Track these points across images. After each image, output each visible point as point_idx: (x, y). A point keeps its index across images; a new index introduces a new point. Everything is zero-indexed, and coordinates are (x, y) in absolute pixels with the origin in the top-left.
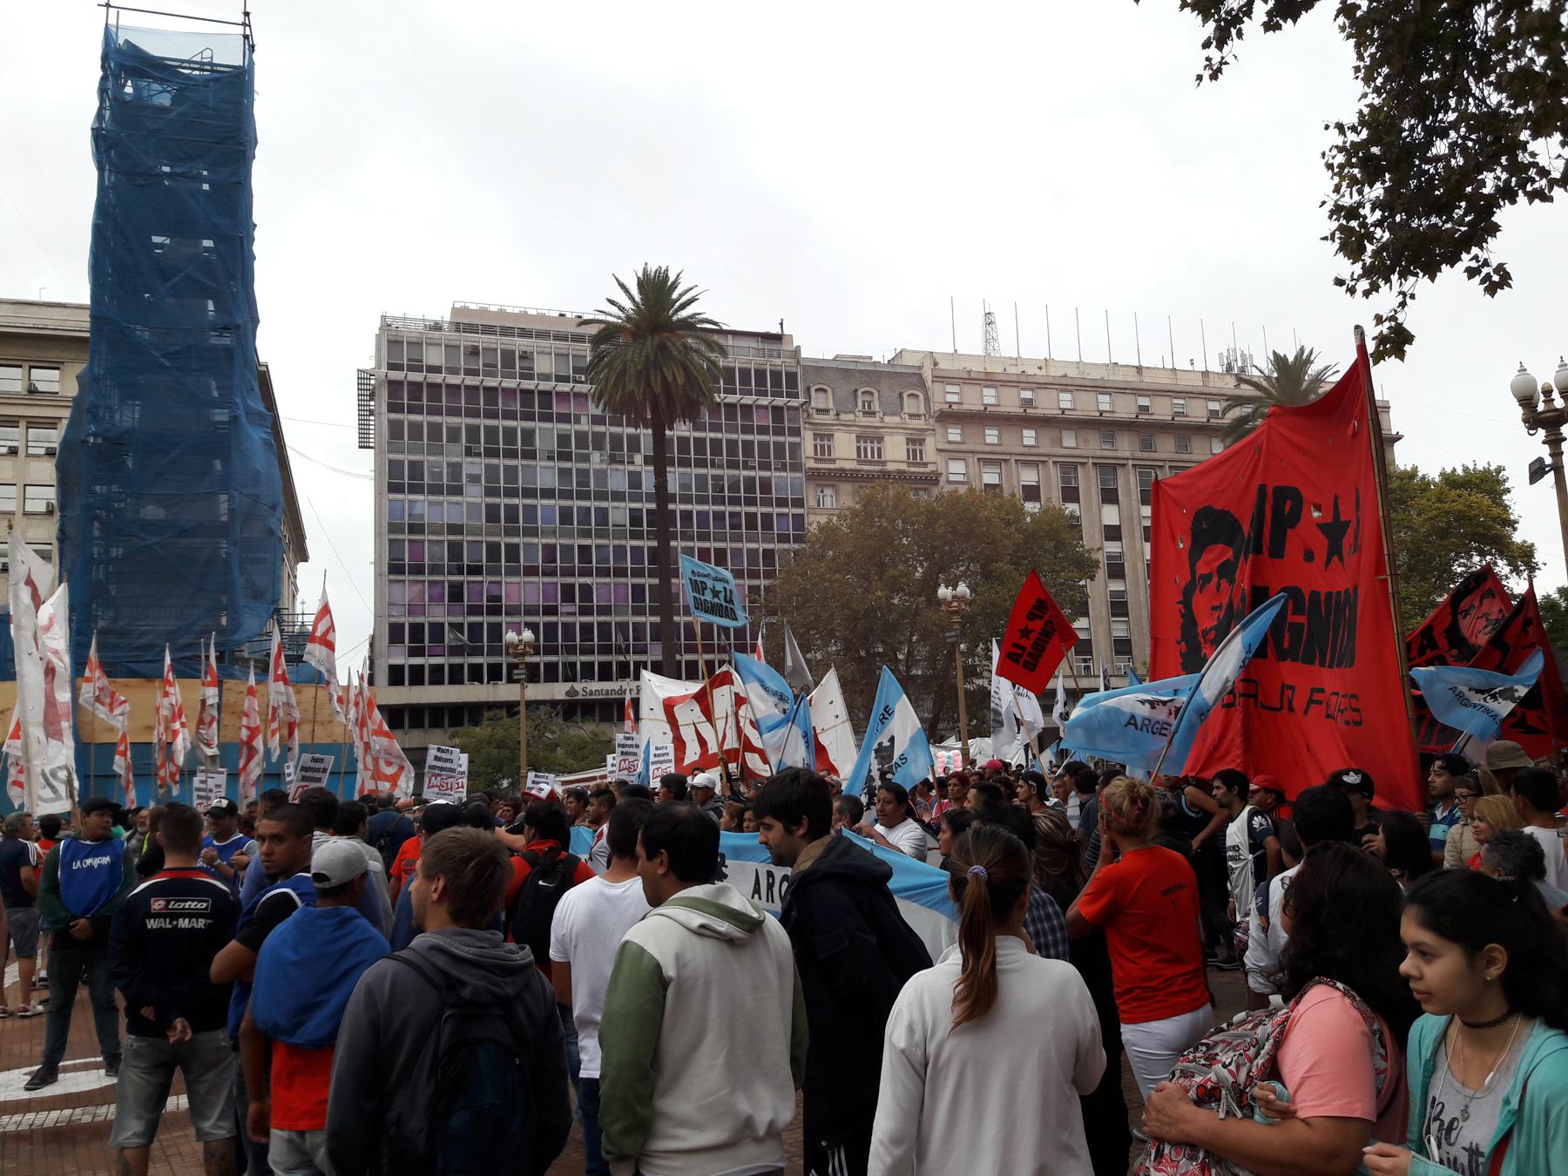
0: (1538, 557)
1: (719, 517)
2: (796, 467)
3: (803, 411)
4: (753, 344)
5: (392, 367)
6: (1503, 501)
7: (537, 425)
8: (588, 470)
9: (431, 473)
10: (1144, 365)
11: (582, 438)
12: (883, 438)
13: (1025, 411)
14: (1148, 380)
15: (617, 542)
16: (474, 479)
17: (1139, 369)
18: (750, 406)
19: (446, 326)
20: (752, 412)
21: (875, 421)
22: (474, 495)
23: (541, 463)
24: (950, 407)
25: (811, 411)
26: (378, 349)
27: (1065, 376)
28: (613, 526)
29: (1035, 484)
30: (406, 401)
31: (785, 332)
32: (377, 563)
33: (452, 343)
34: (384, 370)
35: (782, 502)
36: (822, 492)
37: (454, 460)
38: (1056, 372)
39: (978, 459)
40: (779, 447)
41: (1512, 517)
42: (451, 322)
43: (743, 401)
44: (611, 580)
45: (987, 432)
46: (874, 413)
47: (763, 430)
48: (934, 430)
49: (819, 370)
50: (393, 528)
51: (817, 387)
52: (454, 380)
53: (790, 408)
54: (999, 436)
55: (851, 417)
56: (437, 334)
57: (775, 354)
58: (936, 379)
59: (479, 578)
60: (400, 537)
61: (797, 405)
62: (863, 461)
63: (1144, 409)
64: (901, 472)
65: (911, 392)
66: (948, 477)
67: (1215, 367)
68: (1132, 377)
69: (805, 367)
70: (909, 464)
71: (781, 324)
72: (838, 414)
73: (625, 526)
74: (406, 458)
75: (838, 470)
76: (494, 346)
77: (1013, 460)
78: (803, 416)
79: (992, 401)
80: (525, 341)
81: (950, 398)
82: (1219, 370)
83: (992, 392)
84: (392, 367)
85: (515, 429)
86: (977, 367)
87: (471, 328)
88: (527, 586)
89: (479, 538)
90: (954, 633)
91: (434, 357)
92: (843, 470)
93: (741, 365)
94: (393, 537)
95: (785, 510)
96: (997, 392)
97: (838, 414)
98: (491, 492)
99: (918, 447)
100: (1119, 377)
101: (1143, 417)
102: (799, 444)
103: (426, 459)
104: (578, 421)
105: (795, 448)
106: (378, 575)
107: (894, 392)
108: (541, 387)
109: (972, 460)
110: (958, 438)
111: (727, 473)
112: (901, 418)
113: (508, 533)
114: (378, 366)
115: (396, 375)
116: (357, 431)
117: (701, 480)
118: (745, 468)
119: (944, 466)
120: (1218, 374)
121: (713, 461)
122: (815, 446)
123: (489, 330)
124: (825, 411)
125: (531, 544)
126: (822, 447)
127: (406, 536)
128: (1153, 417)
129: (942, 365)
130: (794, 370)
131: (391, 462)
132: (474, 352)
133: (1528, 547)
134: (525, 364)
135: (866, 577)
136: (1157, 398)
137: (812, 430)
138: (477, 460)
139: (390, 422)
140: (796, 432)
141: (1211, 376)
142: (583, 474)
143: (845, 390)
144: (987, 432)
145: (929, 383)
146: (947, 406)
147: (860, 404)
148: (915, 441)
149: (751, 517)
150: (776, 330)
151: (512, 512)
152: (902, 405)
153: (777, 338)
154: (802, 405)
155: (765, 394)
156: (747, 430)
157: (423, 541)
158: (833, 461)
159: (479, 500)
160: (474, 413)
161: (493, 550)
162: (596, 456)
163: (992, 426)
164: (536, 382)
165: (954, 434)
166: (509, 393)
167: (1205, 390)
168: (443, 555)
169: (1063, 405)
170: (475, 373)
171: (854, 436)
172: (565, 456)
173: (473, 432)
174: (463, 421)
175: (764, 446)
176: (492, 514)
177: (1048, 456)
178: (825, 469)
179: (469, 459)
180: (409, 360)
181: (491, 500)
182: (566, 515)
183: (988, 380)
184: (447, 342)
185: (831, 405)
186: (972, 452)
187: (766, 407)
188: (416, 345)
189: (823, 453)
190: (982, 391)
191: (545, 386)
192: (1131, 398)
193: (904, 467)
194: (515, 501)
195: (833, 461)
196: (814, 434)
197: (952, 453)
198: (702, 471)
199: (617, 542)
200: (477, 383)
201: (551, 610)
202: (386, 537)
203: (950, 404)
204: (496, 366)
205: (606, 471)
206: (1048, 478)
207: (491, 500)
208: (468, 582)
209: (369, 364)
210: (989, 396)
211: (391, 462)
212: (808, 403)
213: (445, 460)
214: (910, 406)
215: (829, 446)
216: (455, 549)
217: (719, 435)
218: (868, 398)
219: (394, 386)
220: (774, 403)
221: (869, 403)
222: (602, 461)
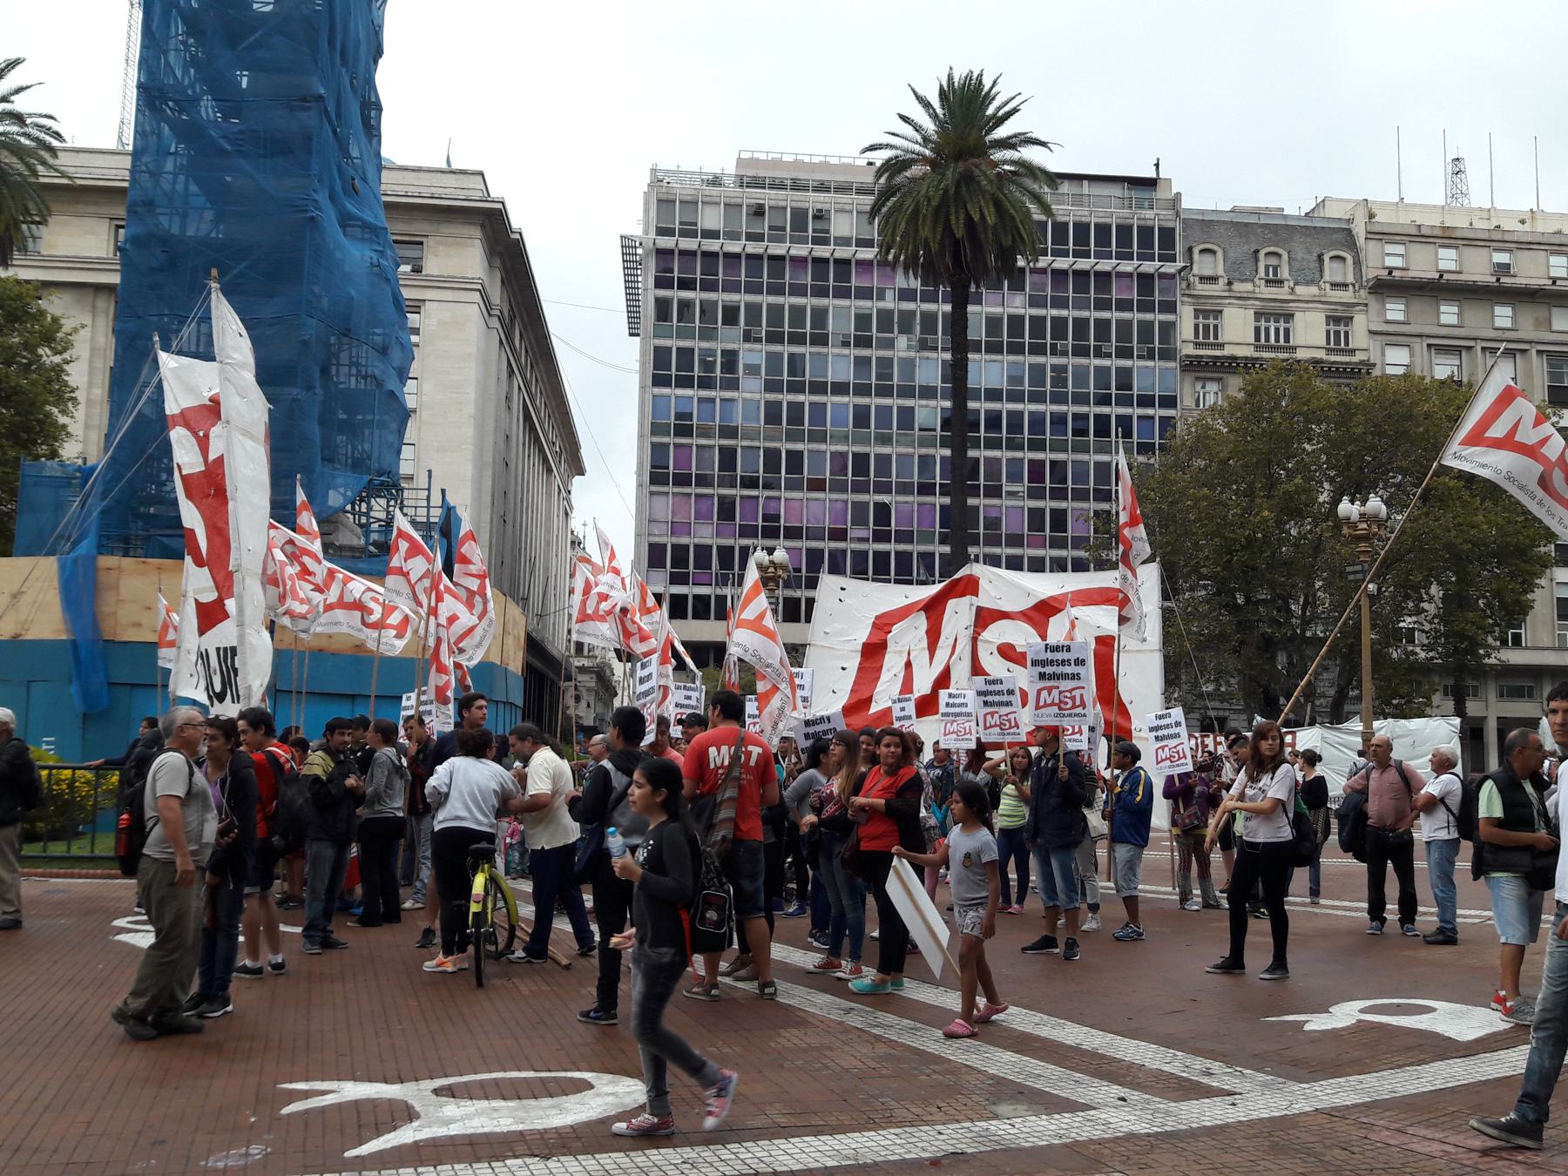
1: (1058, 420)
2: (1168, 354)
4: (1115, 191)
5: (661, 232)
7: (830, 302)
8: (891, 360)
9: (703, 362)
11: (885, 318)
12: (1293, 315)
13: (1498, 280)
15: (924, 451)
16: (752, 370)
18: (1107, 275)
19: (729, 181)
20: (1110, 282)
21: (1282, 293)
22: (751, 391)
23: (832, 350)
24: (1390, 273)
25: (1192, 279)
26: (646, 211)
27: (1559, 233)
28: (921, 430)
30: (698, 276)
32: (639, 473)
33: (733, 201)
34: (652, 235)
35: (1146, 401)
36: (1203, 387)
37: (730, 346)
38: (1544, 227)
39: (1429, 346)
40: (1146, 327)
42: (736, 176)
43: (1099, 268)
44: (914, 499)
45: (1443, 308)
46: (1281, 282)
47: (1124, 305)
48: (1366, 305)
49: (1208, 226)
50: (656, 429)
52: (734, 247)
53: (1163, 276)
54: (1460, 315)
55: (1248, 286)
56: (714, 191)
57: (1146, 204)
59: (754, 493)
60: (665, 440)
61: (1172, 270)
64: (1316, 362)
66: (1384, 369)
70: (1329, 351)
72: (1230, 283)
73: (934, 430)
74: (674, 343)
75: (1228, 358)
76: (783, 204)
77: (1479, 348)
78: (1180, 286)
79: (1452, 266)
80: (822, 196)
81: (1391, 262)
83: (1452, 253)
84: (661, 232)
85: (803, 308)
86: (1431, 221)
87: (757, 183)
88: (811, 503)
89: (756, 444)
90: (1359, 568)
91: (711, 219)
92: (1234, 358)
94: (657, 439)
95: (1150, 412)
97: (1230, 283)
98: (772, 386)
99: (1342, 328)
102: (1173, 324)
103: (697, 344)
104: (881, 297)
105: (1168, 329)
106: (640, 485)
107: (1311, 253)
108: (838, 255)
109: (1420, 346)
110: (1400, 317)
111: (1071, 361)
112: (1320, 288)
113: (791, 437)
114: (646, 232)
115: (666, 242)
116: (625, 315)
117: (1037, 371)
118: (1098, 354)
119: (1379, 353)
121: (1054, 346)
122: (1196, 326)
123: (778, 185)
124: (1213, 279)
125: (818, 451)
126: (1206, 327)
127: (671, 440)
129: (1376, 219)
130: (1170, 225)
131: (657, 349)
132: (758, 212)
134: (820, 226)
135: (1250, 493)
137: (1191, 304)
138: (757, 346)
139: (658, 300)
140: (1170, 307)
142: (885, 364)
143: (1241, 250)
144: (1443, 308)
145: (1361, 241)
146: (1386, 272)
148: (1339, 319)
149: (1103, 421)
150: (1150, 173)
151: (796, 410)
152: (1322, 271)
153: (1150, 183)
154: (1180, 271)
155: (1129, 257)
156: (1103, 305)
157: (690, 446)
159: (757, 396)
160: (754, 288)
161: (772, 457)
162: (902, 342)
163: (1449, 300)
164: (832, 247)
165: (1395, 310)
166: (799, 262)
168: (714, 463)
169: (1554, 273)
170: (757, 238)
171: (1252, 312)
172: (862, 342)
173: (754, 311)
174: (742, 299)
175: (1124, 326)
176: (773, 413)
177: (1530, 342)
178: (1209, 357)
179: (747, 346)
180: (681, 223)
181: (771, 397)
182: (861, 417)
183: (1447, 237)
184: (728, 201)
185: (1220, 271)
186: (1420, 336)
187: (1130, 275)
188: (691, 204)
189: (1207, 335)
191: (843, 253)
193: (1321, 355)
194: (800, 398)
195: (1221, 346)
196: (1195, 310)
197: (1390, 336)
198: (1040, 359)
199: (924, 451)
200: (761, 251)
201: (838, 535)
202: (649, 439)
203: (1391, 271)
204: (784, 229)
205: (913, 360)
206: (1529, 374)
207: (771, 397)
208: (742, 497)
209: (636, 230)
210: (1447, 259)
211: (657, 349)
212: (1188, 268)
213: (718, 346)
214: (1332, 271)
215: (1216, 327)
216: (728, 456)
217: (1064, 313)
218: (1273, 261)
219: (663, 254)
220: (1141, 269)
221: (1275, 269)
222: (909, 347)
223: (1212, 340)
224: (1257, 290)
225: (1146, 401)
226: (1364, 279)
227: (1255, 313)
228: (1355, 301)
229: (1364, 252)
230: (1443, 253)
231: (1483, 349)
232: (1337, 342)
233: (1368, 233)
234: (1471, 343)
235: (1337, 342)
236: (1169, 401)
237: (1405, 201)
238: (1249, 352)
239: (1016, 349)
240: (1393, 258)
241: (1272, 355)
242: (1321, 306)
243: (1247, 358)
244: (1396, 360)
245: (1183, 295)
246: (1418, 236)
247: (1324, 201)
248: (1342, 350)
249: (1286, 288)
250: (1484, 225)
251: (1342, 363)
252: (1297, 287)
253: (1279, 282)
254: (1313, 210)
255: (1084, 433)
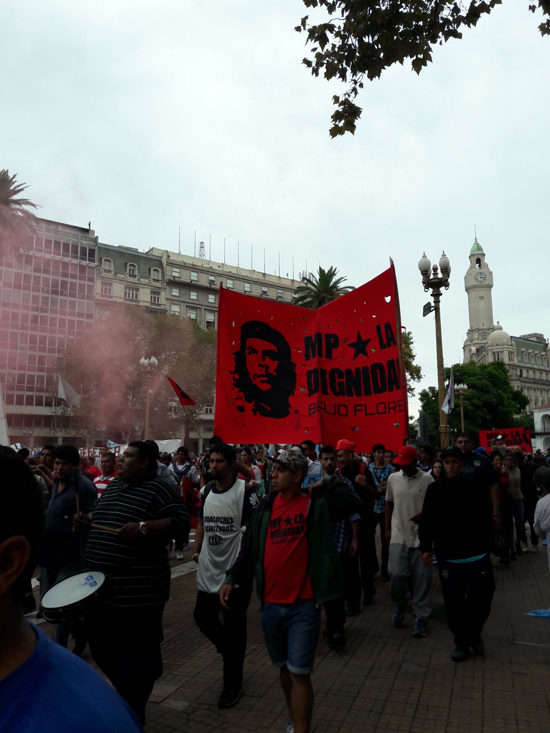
0: (422, 373)
3: (97, 270)
4: (73, 232)
6: (410, 347)
10: (266, 273)
12: (139, 289)
13: (210, 286)
14: (267, 279)
17: (264, 274)
21: (135, 280)
24: (174, 278)
27: (230, 272)
29: (213, 321)
31: (91, 229)
35: (80, 315)
36: (104, 312)
38: (226, 270)
39: (187, 306)
41: (413, 354)
43: (64, 260)
45: (192, 293)
46: (135, 276)
47: (73, 277)
51: (106, 258)
53: (90, 267)
54: (197, 296)
55: (123, 276)
58: (169, 264)
61: (93, 266)
62: (128, 299)
63: (265, 292)
64: (147, 307)
65: (155, 268)
67: (298, 279)
68: (261, 277)
69: (100, 248)
70: (152, 304)
71: (89, 224)
72: (116, 274)
79: (195, 279)
82: (299, 280)
83: (195, 274)
92: (116, 302)
93: (64, 241)
95: (82, 319)
96: (198, 275)
97: (116, 274)
99: (156, 296)
100: (255, 276)
101: (264, 296)
105: (91, 288)
109: (184, 306)
110: (177, 294)
112: (149, 280)
118: (62, 294)
119: (169, 306)
120: (298, 282)
124: (109, 271)
126: (106, 289)
128: (268, 297)
130: (93, 248)
133: (418, 368)
136: (271, 288)
137: (101, 280)
140: (92, 280)
141: (295, 282)
144: (192, 293)
145: (165, 265)
147: (128, 271)
148: (155, 293)
158: (112, 297)
163: (194, 291)
165: (176, 292)
167: (291, 288)
171: (123, 286)
178: (106, 301)
183: (194, 268)
185: (112, 269)
187: (76, 265)
190: (190, 274)
192: (259, 287)
193: (148, 305)
197: (172, 301)
203: (174, 277)
210: (194, 276)
214: (154, 275)
215: (110, 290)
217: (48, 276)
218: (132, 268)
221: (133, 271)
223: (108, 294)
224: (126, 278)
225: (80, 315)
226: (165, 279)
227: (125, 286)
228: (161, 287)
229: (165, 270)
230: (193, 274)
231: (205, 309)
232: (155, 301)
233: (167, 262)
234: (201, 307)
235: (155, 301)
236: (90, 316)
237: (181, 253)
238: (122, 301)
239: (26, 288)
240: (176, 273)
241: (131, 303)
242: (149, 287)
243: (121, 303)
244: (175, 309)
245: (98, 276)
246: (184, 266)
247: (152, 249)
248: (156, 304)
249: (137, 279)
250: (207, 266)
251: (156, 309)
252: (141, 279)
253: (135, 276)
254: (148, 251)
255: (55, 325)
